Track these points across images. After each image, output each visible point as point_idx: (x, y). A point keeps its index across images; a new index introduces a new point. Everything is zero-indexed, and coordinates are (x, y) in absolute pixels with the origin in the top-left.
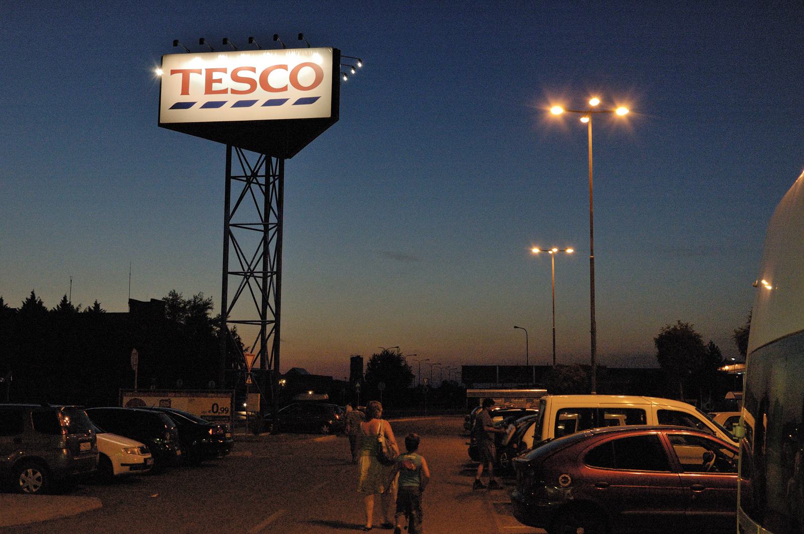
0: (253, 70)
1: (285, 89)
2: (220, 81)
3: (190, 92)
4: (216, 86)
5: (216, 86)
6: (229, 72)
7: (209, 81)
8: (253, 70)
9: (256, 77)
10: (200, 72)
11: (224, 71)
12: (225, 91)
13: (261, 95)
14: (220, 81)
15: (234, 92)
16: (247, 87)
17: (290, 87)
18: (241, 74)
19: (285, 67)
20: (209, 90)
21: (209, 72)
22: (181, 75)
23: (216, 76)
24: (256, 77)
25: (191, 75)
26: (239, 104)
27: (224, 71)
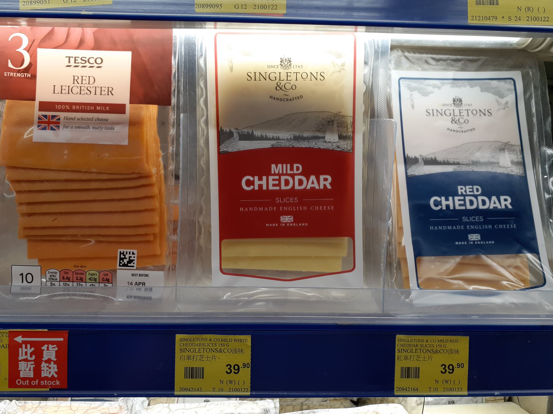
0: (86, 58)
1: (93, 64)
2: (77, 60)
3: (71, 62)
4: (77, 62)
5: (77, 62)
6: (80, 58)
7: (75, 60)
8: (86, 58)
9: (87, 60)
10: (72, 57)
11: (79, 57)
12: (79, 63)
13: (87, 64)
14: (77, 60)
15: (81, 63)
16: (84, 62)
17: (95, 63)
18: (83, 59)
19: (93, 58)
20: (75, 63)
21: (75, 58)
22: (68, 58)
23: (77, 59)
24: (87, 60)
25: (71, 58)
26: (83, 67)
27: (79, 57)
